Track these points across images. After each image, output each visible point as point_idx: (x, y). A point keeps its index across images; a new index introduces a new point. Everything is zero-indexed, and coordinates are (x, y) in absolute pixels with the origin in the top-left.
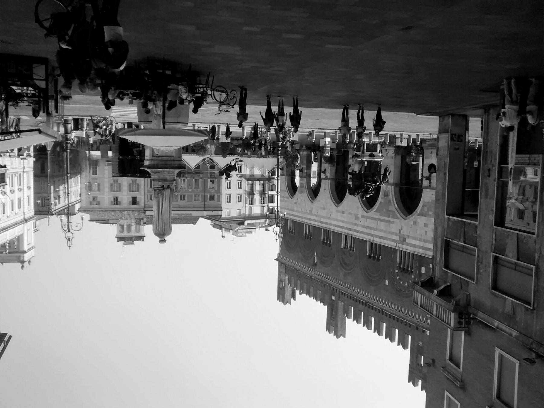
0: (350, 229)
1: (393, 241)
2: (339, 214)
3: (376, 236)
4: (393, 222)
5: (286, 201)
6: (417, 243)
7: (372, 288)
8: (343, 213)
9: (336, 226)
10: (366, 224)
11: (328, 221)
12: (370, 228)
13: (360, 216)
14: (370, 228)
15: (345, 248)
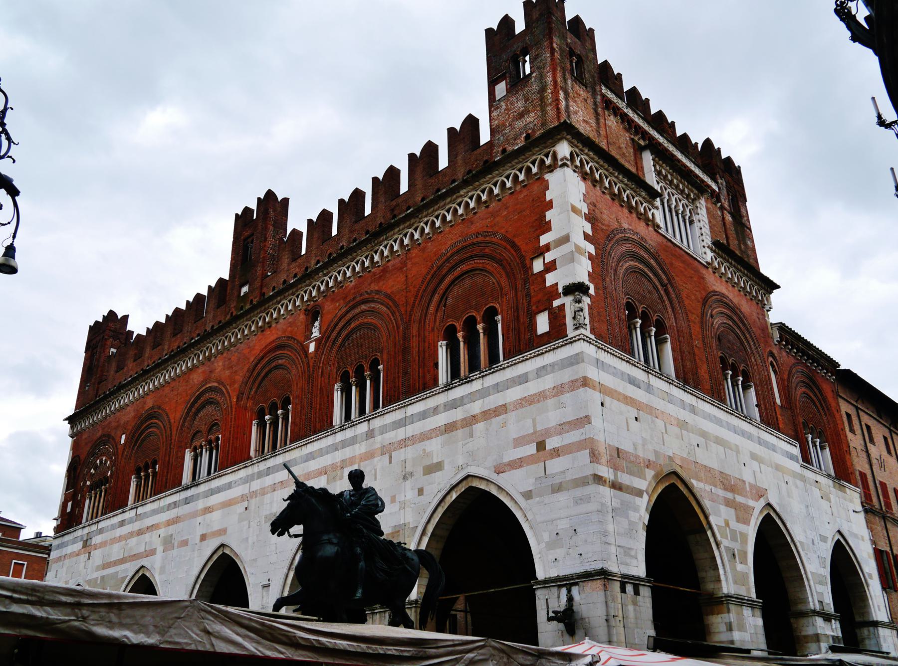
0: (187, 501)
1: (101, 531)
2: (216, 527)
3: (131, 521)
4: (98, 568)
5: (519, 442)
6: (70, 549)
7: (150, 403)
8: (203, 538)
9: (229, 486)
10: (147, 537)
11: (256, 485)
12: (140, 533)
13: (160, 549)
14: (140, 533)
15: (218, 439)
